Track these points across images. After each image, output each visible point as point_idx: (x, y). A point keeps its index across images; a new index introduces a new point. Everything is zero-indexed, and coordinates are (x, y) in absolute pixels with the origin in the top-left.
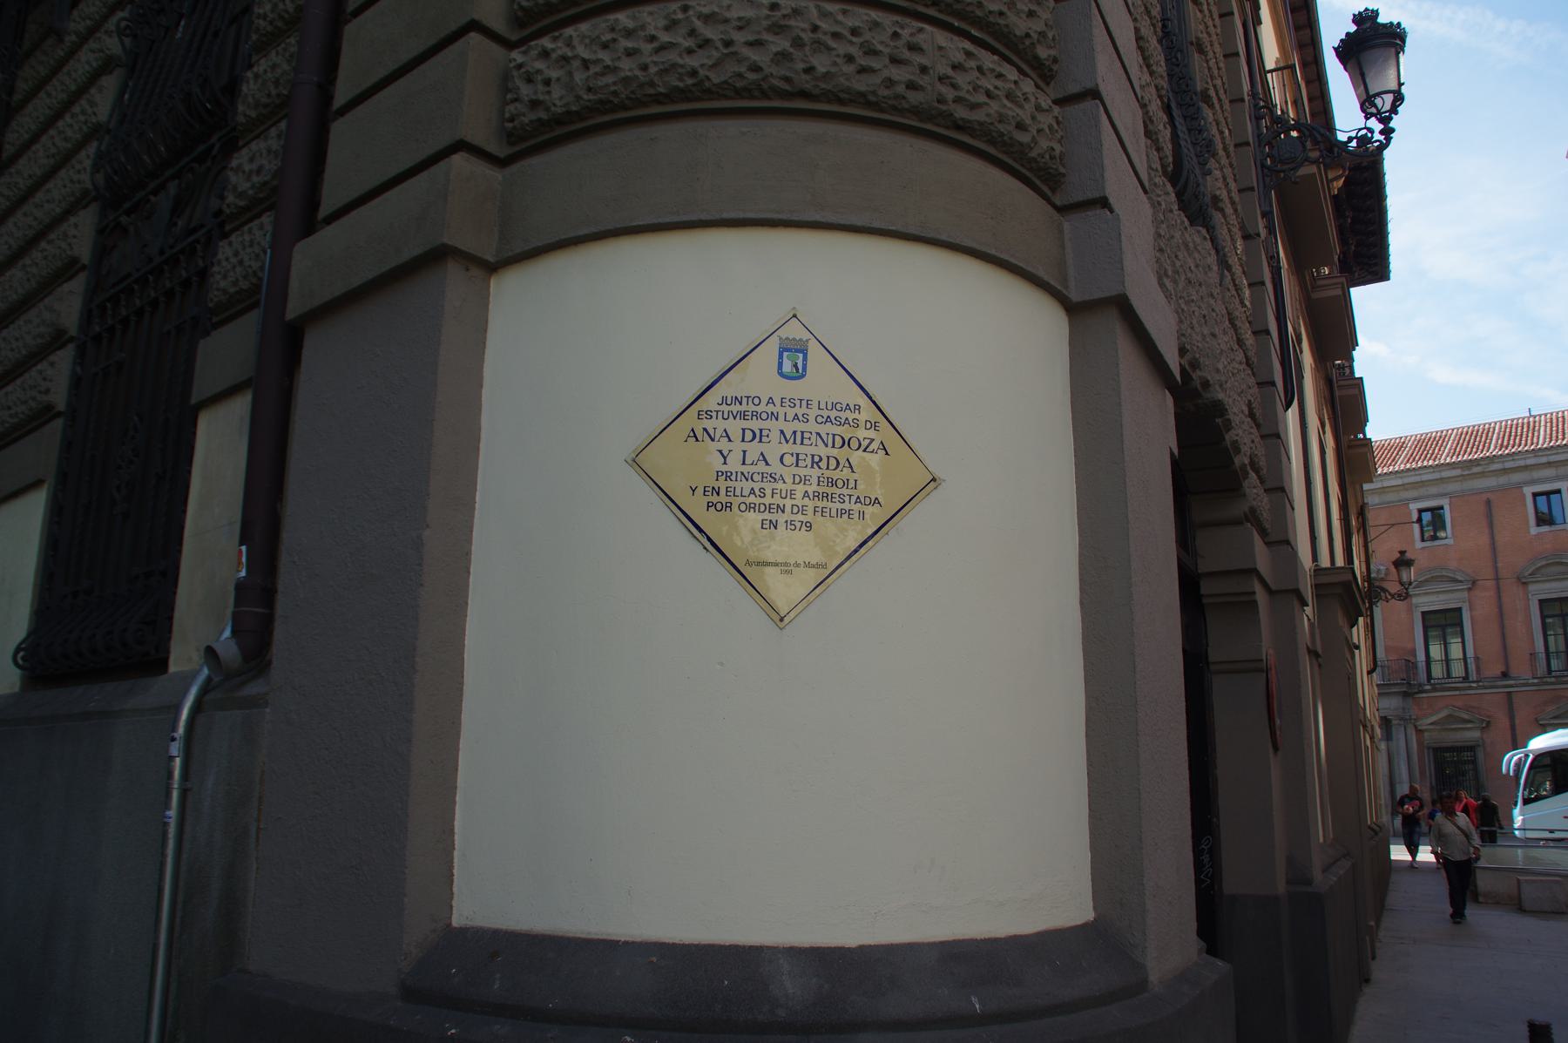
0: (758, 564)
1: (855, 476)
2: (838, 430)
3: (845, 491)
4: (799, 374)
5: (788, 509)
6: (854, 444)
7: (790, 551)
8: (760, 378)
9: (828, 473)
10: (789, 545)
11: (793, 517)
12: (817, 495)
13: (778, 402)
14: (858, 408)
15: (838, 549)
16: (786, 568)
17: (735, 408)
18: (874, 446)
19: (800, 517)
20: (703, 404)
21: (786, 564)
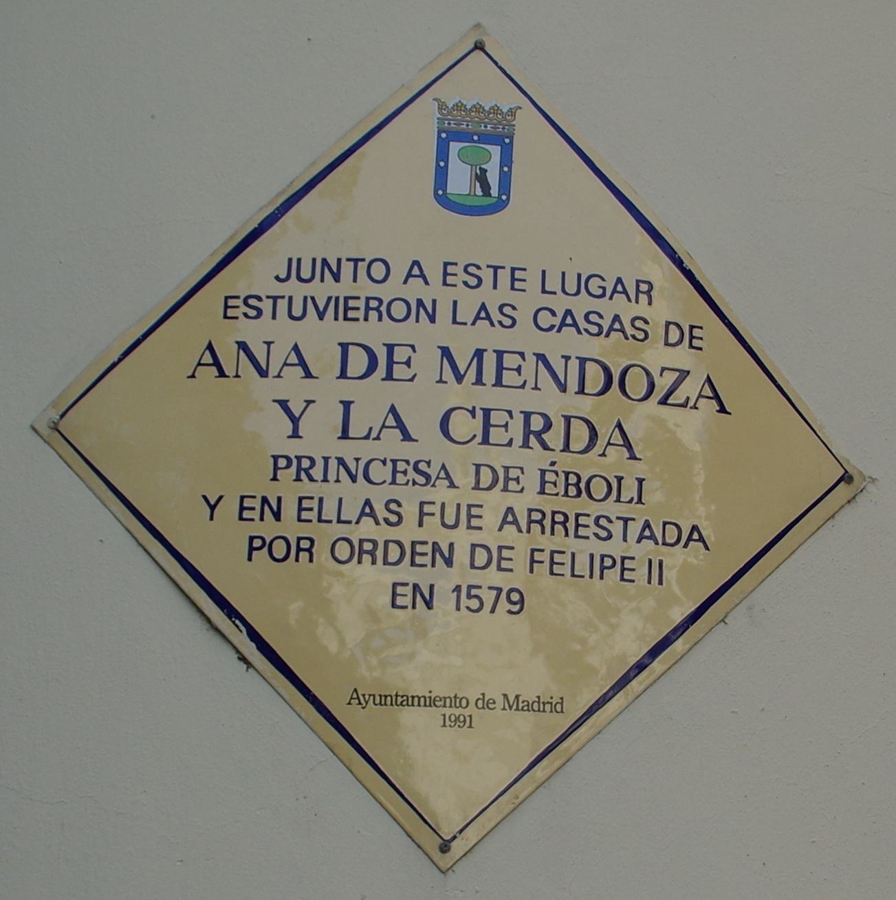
0: (384, 700)
1: (640, 469)
2: (592, 347)
3: (611, 509)
4: (490, 200)
5: (462, 556)
6: (637, 384)
7: (468, 666)
8: (388, 211)
9: (567, 462)
10: (462, 650)
11: (475, 577)
12: (537, 519)
13: (434, 274)
14: (646, 289)
15: (594, 660)
16: (456, 710)
17: (323, 290)
18: (689, 389)
19: (494, 577)
20: (235, 280)
21: (456, 701)
